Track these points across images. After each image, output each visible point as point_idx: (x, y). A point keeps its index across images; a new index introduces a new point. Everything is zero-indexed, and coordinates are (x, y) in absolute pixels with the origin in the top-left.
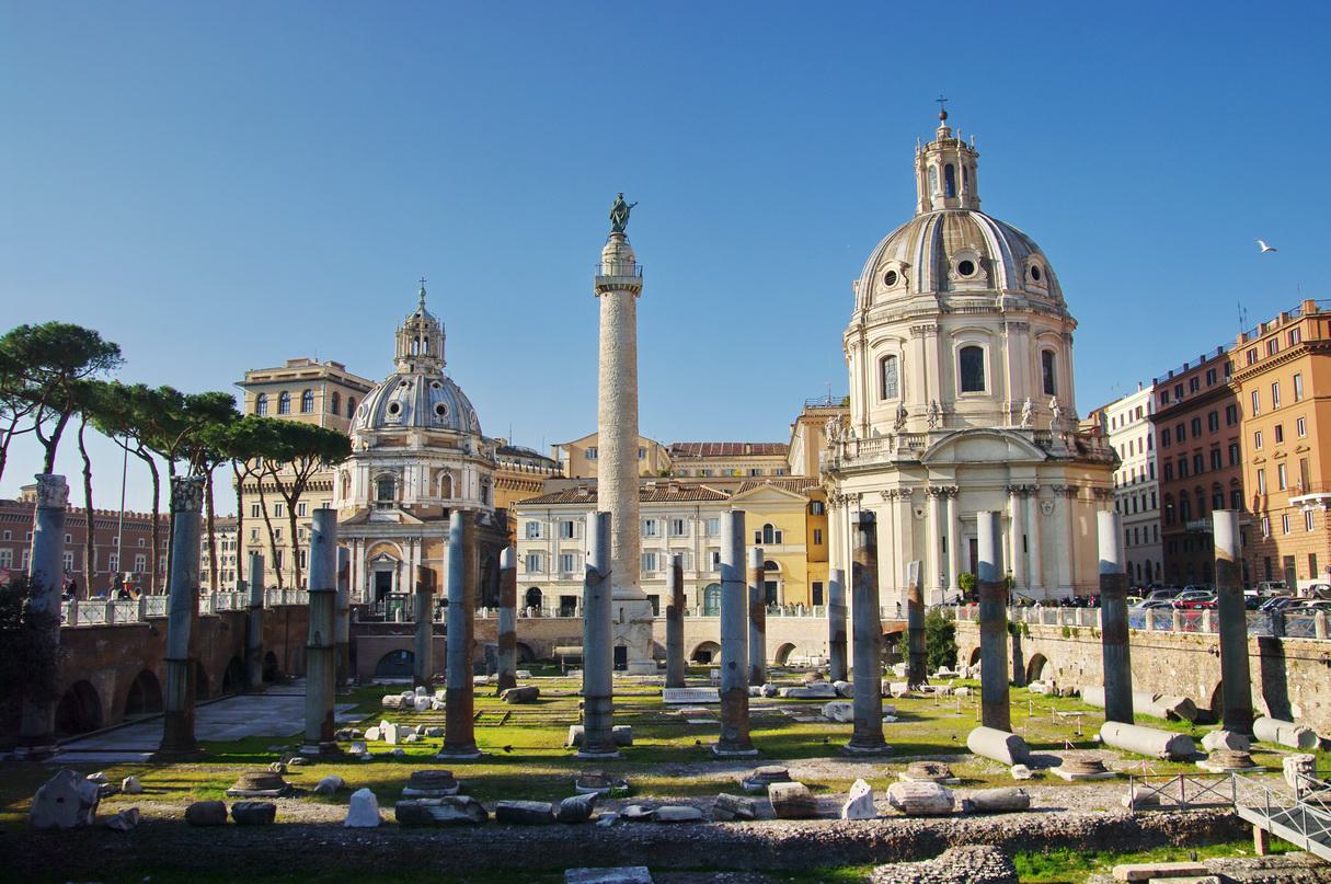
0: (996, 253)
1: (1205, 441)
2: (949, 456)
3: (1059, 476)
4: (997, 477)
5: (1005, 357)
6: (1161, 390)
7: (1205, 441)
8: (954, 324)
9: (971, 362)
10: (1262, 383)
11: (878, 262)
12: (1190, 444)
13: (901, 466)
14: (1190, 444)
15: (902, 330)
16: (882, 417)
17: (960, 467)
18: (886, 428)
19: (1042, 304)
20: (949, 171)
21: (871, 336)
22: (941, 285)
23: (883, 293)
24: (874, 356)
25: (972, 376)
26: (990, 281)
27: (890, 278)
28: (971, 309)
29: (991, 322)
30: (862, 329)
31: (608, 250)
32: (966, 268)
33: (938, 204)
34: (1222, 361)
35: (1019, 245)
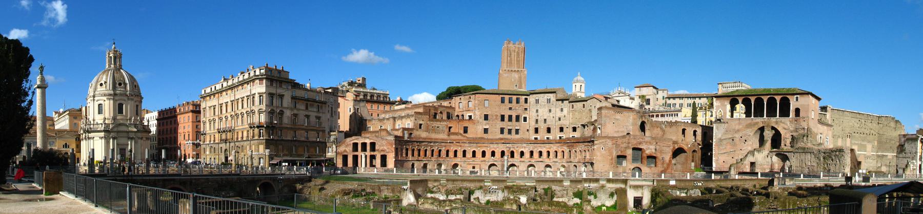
0: (127, 81)
1: (169, 127)
2: (115, 129)
3: (139, 135)
4: (125, 134)
5: (128, 108)
6: (160, 113)
7: (169, 127)
8: (117, 98)
9: (120, 106)
10: (182, 116)
11: (97, 81)
12: (165, 127)
13: (104, 131)
14: (165, 127)
15: (105, 98)
16: (99, 119)
17: (118, 132)
18: (101, 122)
19: (136, 96)
20: (115, 58)
21: (96, 99)
22: (114, 88)
23: (99, 88)
24: (97, 104)
25: (120, 111)
26: (125, 88)
27: (101, 85)
28: (121, 95)
29: (126, 98)
30: (94, 97)
31: (39, 77)
32: (120, 84)
33: (112, 66)
34: (174, 109)
35: (132, 79)
